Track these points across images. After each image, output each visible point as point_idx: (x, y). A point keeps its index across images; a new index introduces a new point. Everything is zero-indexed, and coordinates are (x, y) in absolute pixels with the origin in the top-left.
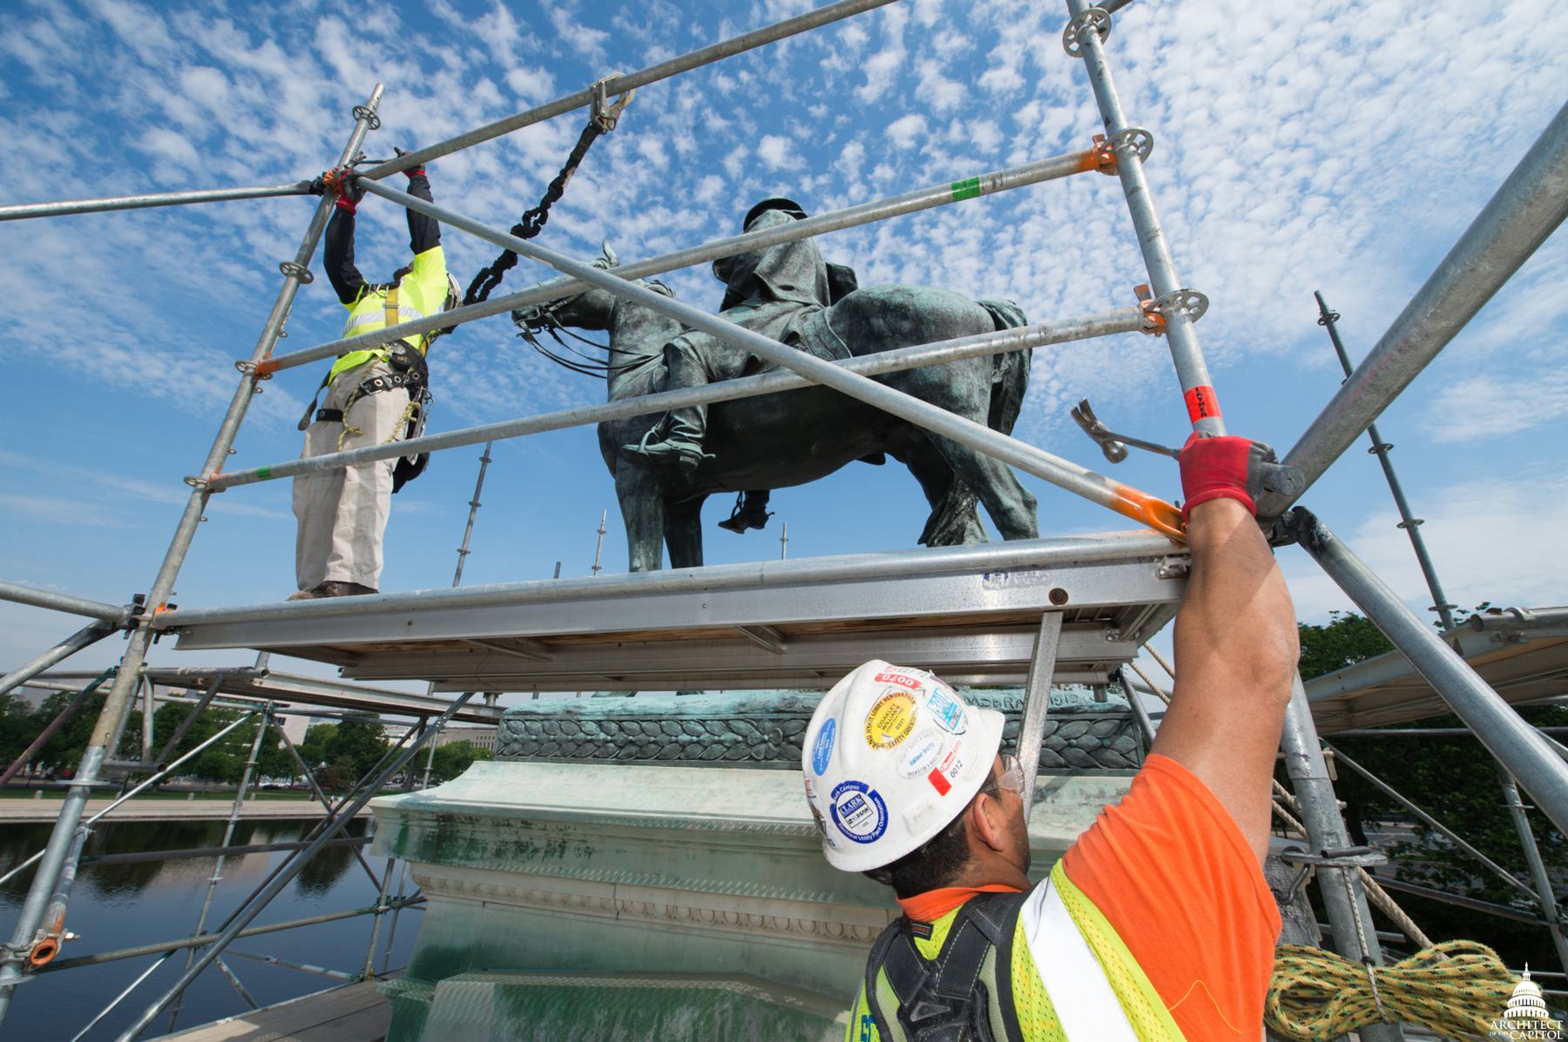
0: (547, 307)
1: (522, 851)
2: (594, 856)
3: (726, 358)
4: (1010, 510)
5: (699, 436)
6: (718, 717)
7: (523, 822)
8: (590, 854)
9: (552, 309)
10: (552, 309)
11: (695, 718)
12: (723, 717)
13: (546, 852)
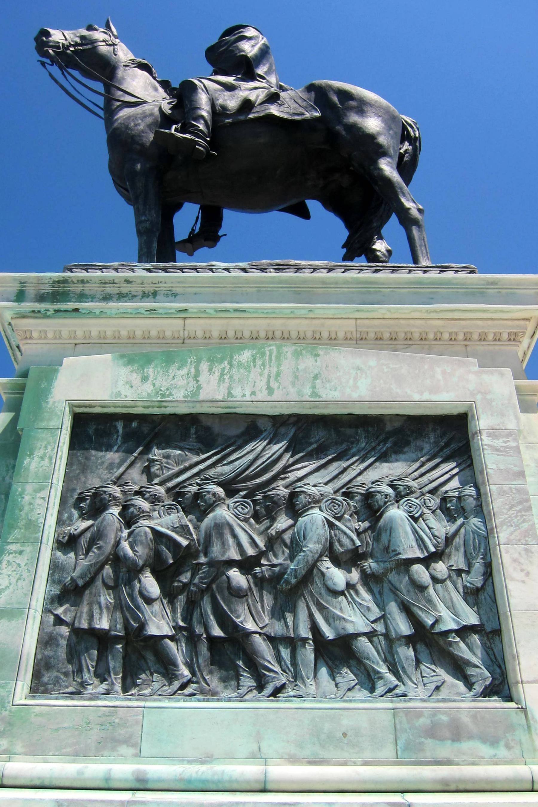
1: (123, 297)
2: (178, 297)
3: (225, 100)
4: (409, 209)
5: (208, 139)
6: (238, 267)
7: (126, 281)
8: (175, 296)
11: (222, 267)
12: (242, 267)
13: (143, 297)
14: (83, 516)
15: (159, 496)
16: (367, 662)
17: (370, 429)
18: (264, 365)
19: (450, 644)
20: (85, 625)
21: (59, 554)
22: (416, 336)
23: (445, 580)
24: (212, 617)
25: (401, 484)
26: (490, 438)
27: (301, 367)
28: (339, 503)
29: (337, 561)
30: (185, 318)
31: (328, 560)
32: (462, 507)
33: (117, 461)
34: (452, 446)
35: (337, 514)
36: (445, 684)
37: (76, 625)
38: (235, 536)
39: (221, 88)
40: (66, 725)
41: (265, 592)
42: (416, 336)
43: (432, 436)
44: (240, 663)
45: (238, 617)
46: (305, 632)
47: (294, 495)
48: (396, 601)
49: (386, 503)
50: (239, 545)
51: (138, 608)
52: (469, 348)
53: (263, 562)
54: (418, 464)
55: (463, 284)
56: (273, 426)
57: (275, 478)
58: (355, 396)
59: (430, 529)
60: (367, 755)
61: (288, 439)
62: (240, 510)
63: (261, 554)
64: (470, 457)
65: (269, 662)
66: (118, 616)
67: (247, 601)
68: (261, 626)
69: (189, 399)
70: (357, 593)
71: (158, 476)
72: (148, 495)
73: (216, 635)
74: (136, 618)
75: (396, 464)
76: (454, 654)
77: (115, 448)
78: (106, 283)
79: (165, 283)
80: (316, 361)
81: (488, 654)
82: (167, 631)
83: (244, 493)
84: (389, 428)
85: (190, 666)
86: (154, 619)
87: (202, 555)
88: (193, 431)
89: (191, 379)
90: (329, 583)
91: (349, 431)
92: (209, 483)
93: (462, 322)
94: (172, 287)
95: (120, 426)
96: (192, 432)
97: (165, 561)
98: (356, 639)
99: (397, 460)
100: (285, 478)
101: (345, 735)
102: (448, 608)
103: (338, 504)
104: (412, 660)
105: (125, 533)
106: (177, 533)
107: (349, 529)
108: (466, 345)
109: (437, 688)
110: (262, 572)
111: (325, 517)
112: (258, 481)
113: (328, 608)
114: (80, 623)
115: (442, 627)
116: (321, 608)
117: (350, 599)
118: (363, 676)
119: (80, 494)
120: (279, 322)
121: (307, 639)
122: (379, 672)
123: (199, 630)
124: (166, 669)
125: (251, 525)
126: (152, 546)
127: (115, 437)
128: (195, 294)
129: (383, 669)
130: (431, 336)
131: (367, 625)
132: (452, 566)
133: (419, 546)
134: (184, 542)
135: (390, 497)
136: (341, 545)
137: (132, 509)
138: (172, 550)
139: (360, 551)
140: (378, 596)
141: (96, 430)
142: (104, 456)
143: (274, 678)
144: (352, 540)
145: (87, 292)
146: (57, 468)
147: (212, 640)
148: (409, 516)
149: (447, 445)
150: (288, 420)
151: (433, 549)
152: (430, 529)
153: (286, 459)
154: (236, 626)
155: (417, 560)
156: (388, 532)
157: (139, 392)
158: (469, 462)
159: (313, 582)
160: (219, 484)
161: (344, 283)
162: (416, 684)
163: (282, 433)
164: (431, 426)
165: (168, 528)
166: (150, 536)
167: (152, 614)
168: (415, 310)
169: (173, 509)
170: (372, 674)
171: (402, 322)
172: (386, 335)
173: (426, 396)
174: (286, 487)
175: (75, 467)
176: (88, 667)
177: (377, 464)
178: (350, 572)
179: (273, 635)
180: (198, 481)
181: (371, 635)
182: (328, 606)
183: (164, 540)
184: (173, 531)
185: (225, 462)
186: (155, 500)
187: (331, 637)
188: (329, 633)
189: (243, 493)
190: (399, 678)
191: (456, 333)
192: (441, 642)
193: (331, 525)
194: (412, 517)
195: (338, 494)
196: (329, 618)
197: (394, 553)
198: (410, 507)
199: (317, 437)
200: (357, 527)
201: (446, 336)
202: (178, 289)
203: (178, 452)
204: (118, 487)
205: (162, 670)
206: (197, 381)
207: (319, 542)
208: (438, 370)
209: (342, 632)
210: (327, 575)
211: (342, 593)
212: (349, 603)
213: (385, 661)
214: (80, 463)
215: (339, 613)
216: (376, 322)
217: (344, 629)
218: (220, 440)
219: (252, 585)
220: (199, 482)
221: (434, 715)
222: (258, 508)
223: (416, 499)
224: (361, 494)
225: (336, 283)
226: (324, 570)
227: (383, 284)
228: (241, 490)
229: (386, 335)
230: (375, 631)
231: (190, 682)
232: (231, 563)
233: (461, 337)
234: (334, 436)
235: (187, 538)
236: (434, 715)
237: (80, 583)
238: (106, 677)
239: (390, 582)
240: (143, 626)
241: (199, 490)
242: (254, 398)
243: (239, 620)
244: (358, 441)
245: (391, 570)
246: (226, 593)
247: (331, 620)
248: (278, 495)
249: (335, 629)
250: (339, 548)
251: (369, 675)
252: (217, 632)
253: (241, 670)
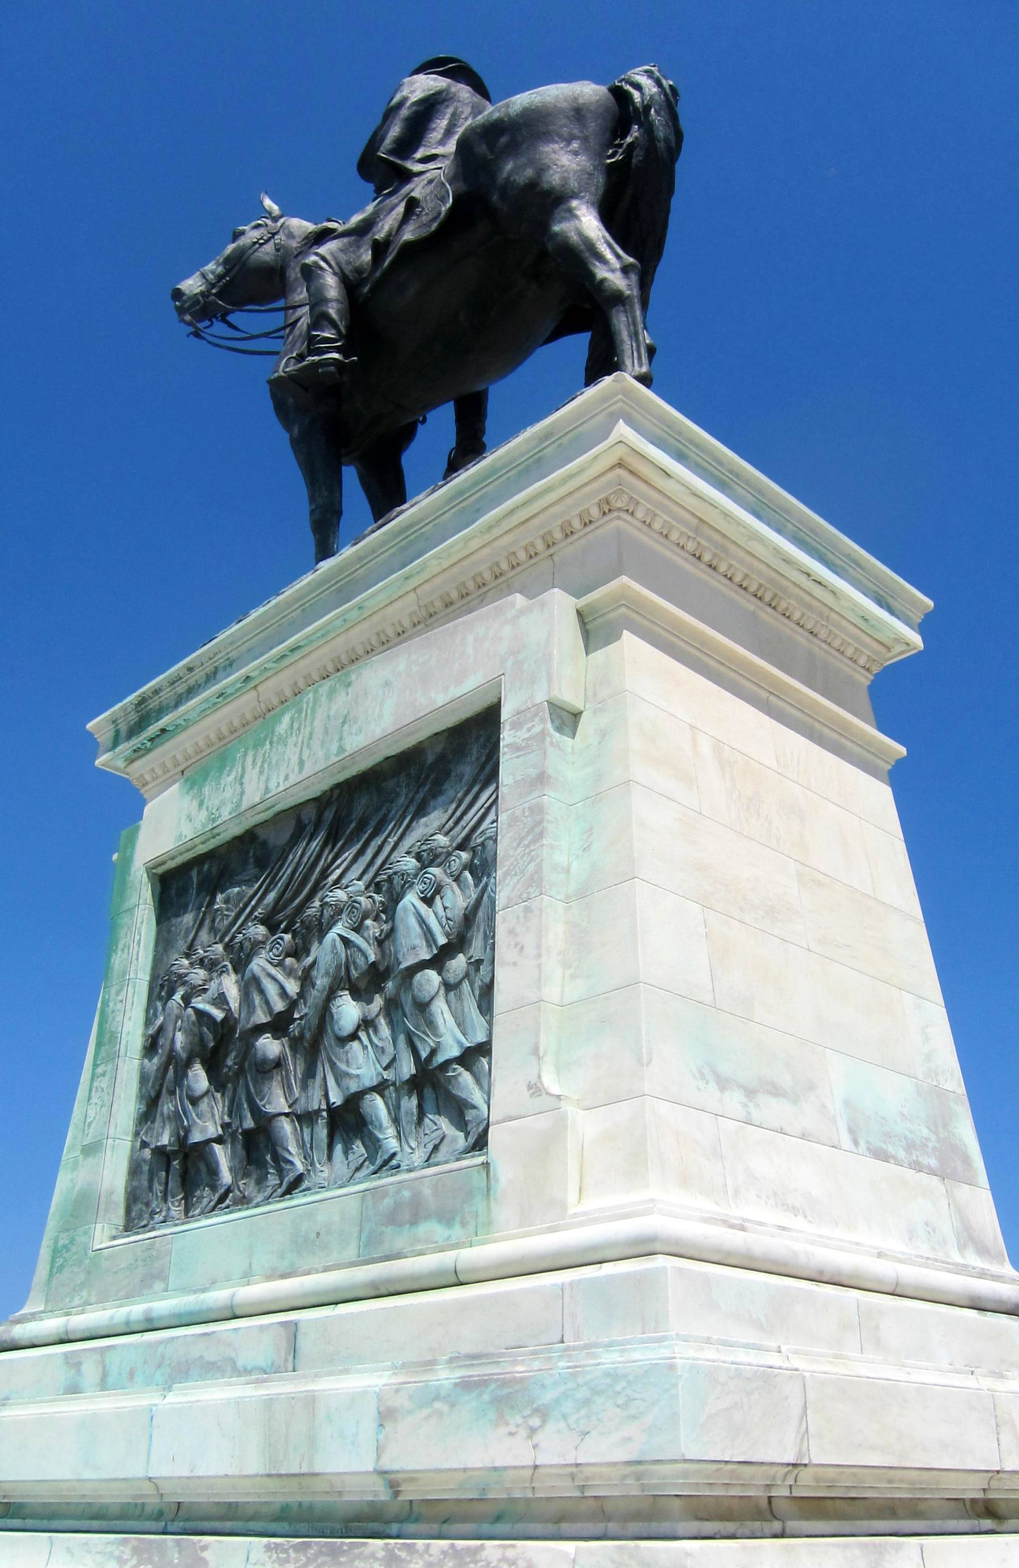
0: (209, 291)
9: (214, 291)
10: (214, 291)
15: (215, 959)
18: (299, 729)
21: (146, 1061)
22: (487, 576)
23: (460, 982)
24: (245, 1106)
26: (513, 731)
27: (332, 713)
29: (356, 994)
30: (256, 686)
31: (347, 992)
36: (446, 1141)
38: (262, 992)
39: (353, 238)
40: (122, 1266)
41: (298, 1056)
42: (487, 576)
43: (475, 751)
44: (268, 1157)
45: (261, 1100)
48: (404, 1032)
49: (403, 886)
50: (267, 1002)
52: (555, 558)
54: (454, 806)
55: (511, 462)
58: (378, 733)
60: (333, 1259)
61: (326, 827)
63: (293, 1005)
67: (282, 1073)
69: (233, 815)
70: (376, 1031)
75: (432, 816)
77: (190, 908)
78: (174, 682)
79: (220, 652)
80: (347, 694)
83: (284, 923)
84: (430, 758)
86: (198, 1121)
89: (237, 784)
93: (535, 522)
94: (228, 653)
98: (362, 1098)
99: (435, 809)
100: (326, 884)
101: (318, 1234)
102: (459, 1025)
104: (412, 1114)
108: (551, 555)
109: (436, 1148)
111: (339, 935)
115: (440, 1059)
120: (340, 640)
126: (196, 1030)
128: (249, 651)
130: (504, 566)
132: (472, 957)
134: (219, 1015)
135: (408, 875)
138: (212, 1029)
139: (382, 968)
142: (182, 921)
143: (289, 1169)
145: (164, 704)
146: (135, 957)
150: (331, 796)
151: (442, 940)
153: (327, 856)
155: (423, 965)
157: (195, 825)
161: (382, 546)
166: (194, 1018)
167: (197, 1115)
168: (467, 540)
171: (465, 563)
172: (454, 595)
173: (455, 692)
177: (414, 824)
178: (369, 1002)
181: (380, 1088)
183: (205, 1019)
187: (339, 1103)
191: (532, 544)
195: (371, 889)
196: (340, 1077)
200: (377, 935)
201: (522, 556)
202: (233, 653)
203: (237, 890)
206: (242, 784)
207: (327, 973)
208: (470, 638)
210: (335, 1017)
211: (354, 1036)
212: (365, 1048)
216: (437, 581)
219: (287, 1050)
221: (398, 1192)
225: (373, 552)
227: (422, 520)
228: (281, 922)
229: (454, 595)
230: (386, 1080)
232: (259, 1030)
233: (540, 546)
235: (223, 1010)
236: (398, 1192)
242: (288, 784)
243: (262, 1103)
244: (398, 795)
246: (254, 1071)
253: (269, 1166)
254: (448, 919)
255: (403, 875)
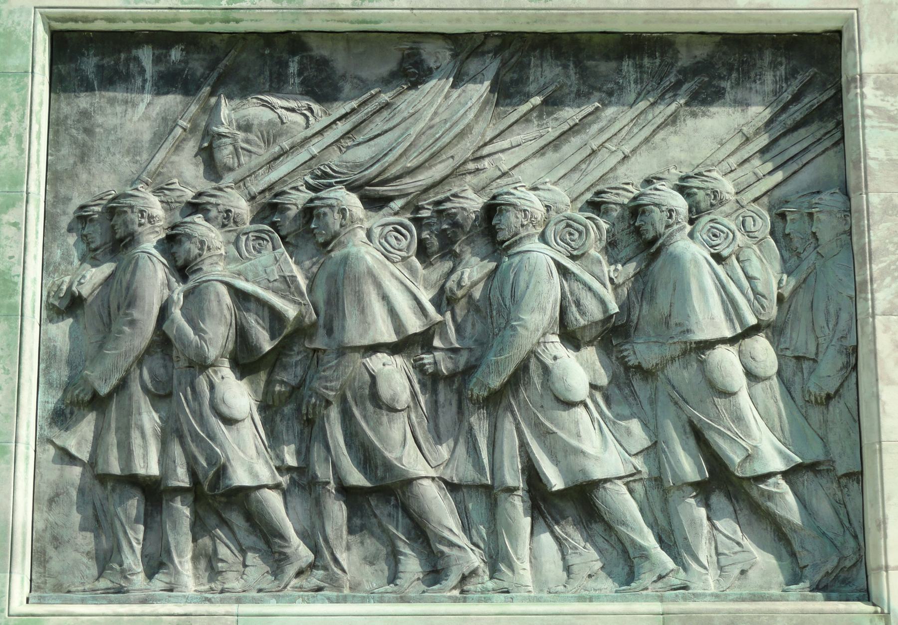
14: (91, 257)
16: (623, 529)
17: (646, 61)
19: (770, 496)
20: (115, 468)
25: (701, 185)
28: (581, 228)
32: (814, 234)
33: (147, 136)
34: (806, 100)
35: (575, 249)
37: (100, 469)
38: (385, 298)
43: (769, 77)
46: (513, 476)
47: (492, 210)
50: (393, 313)
51: (213, 438)
53: (437, 343)
56: (455, 56)
57: (456, 173)
59: (749, 278)
62: (393, 242)
64: (840, 125)
65: (451, 530)
66: (177, 450)
68: (434, 463)
71: (231, 169)
72: (213, 213)
73: (355, 484)
74: (212, 458)
76: (775, 514)
81: (837, 513)
82: (265, 474)
84: (684, 60)
85: (307, 537)
87: (322, 331)
88: (293, 68)
90: (558, 386)
91: (605, 67)
92: (330, 185)
95: (146, 55)
96: (291, 70)
97: (256, 348)
102: (772, 430)
103: (577, 230)
105: (179, 290)
106: (275, 291)
107: (598, 279)
110: (435, 363)
111: (552, 258)
112: (425, 178)
113: (554, 433)
114: (107, 462)
115: (760, 469)
116: (544, 434)
117: (596, 414)
118: (615, 553)
119: (82, 208)
121: (516, 489)
122: (641, 548)
123: (323, 472)
124: (268, 543)
125: (412, 271)
127: (139, 82)
129: (649, 540)
131: (624, 461)
133: (727, 313)
134: (291, 311)
135: (678, 213)
136: (583, 313)
137: (187, 245)
140: (647, 407)
141: (100, 68)
144: (603, 302)
147: (346, 492)
148: (713, 255)
149: (796, 98)
151: (752, 320)
152: (749, 278)
154: (389, 466)
156: (671, 287)
158: (838, 136)
159: (528, 383)
160: (352, 188)
162: (705, 568)
163: (472, 73)
164: (768, 56)
165: (258, 284)
169: (263, 239)
170: (631, 551)
174: (479, 191)
175: (65, 151)
176: (130, 543)
179: (456, 481)
180: (308, 179)
181: (630, 480)
182: (555, 429)
184: (267, 288)
185: (360, 138)
186: (228, 219)
188: (556, 481)
189: (397, 204)
190: (676, 558)
192: (755, 493)
193: (564, 271)
194: (719, 258)
197: (679, 329)
198: (715, 235)
199: (542, 81)
204: (162, 202)
205: (261, 545)
209: (581, 479)
213: (653, 525)
214: (74, 141)
215: (574, 442)
217: (584, 471)
218: (347, 88)
220: (311, 181)
222: (425, 235)
223: (728, 215)
224: (622, 205)
226: (549, 361)
228: (391, 199)
231: (312, 566)
234: (574, 78)
237: (104, 390)
238: (165, 560)
239: (669, 381)
240: (222, 471)
241: (311, 200)
244: (621, 88)
245: (673, 359)
247: (560, 456)
248: (464, 209)
249: (565, 472)
250: (578, 317)
251: (625, 551)
252: (356, 478)
254: (756, 293)
255: (670, 211)
